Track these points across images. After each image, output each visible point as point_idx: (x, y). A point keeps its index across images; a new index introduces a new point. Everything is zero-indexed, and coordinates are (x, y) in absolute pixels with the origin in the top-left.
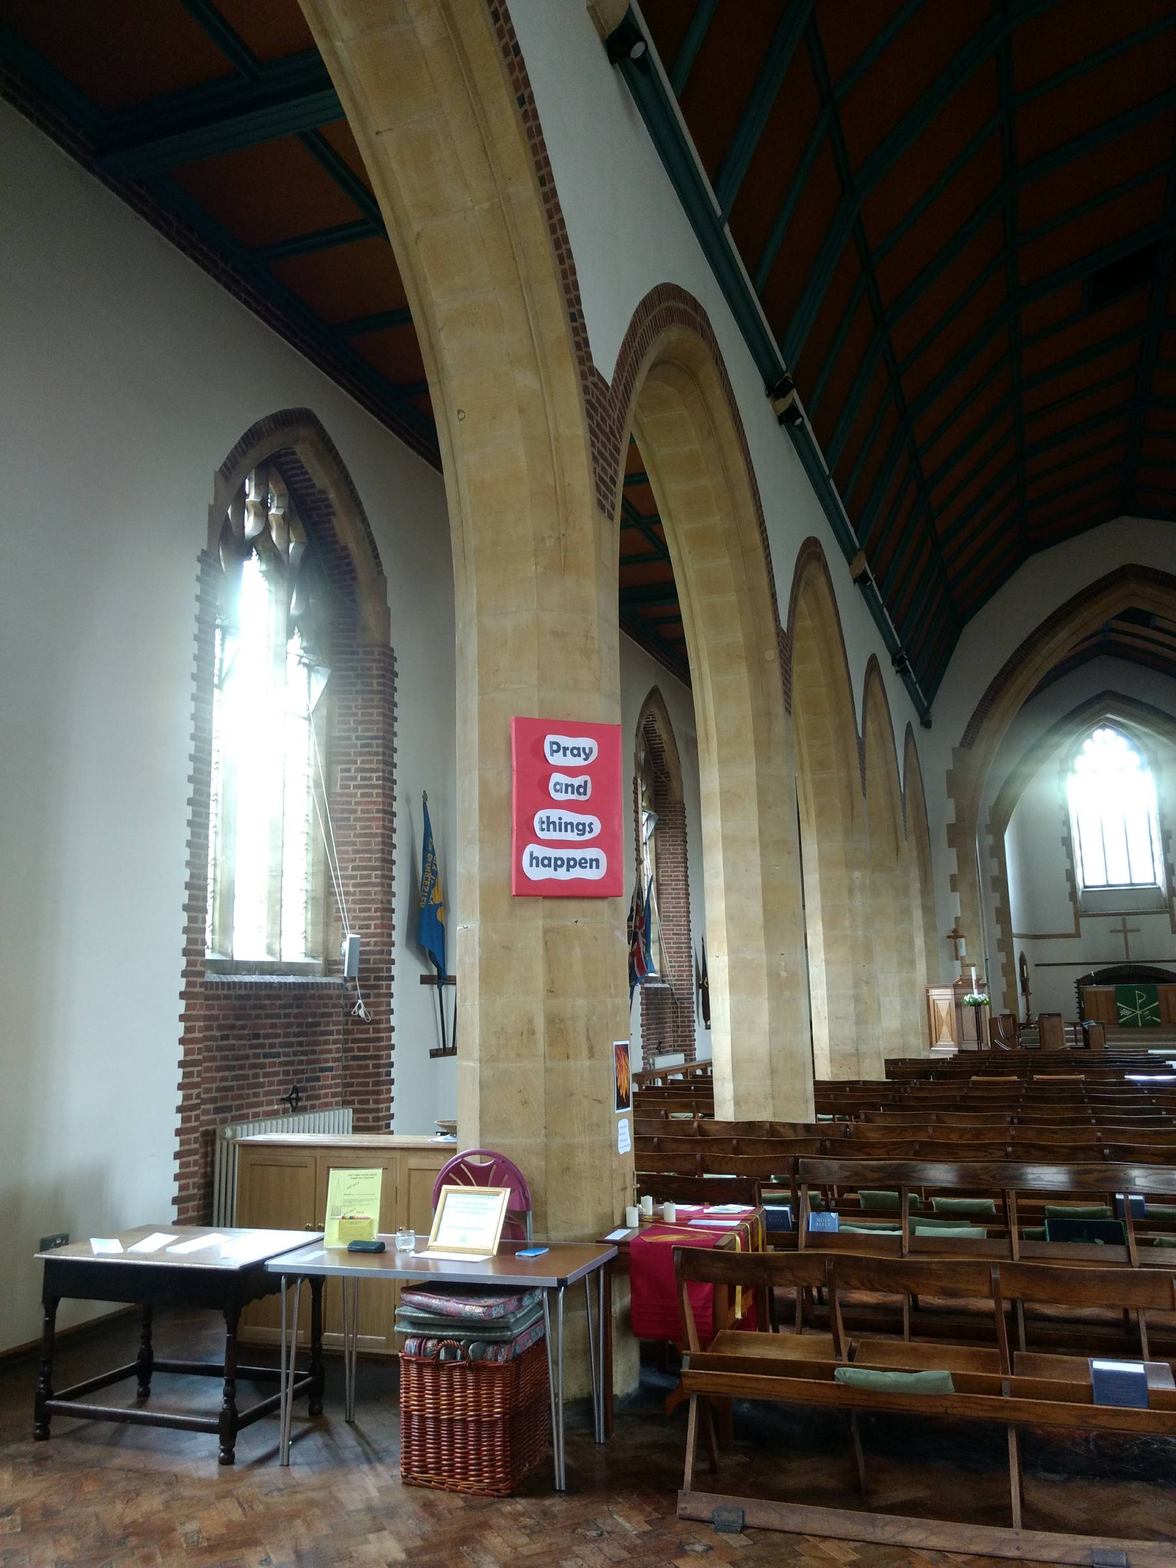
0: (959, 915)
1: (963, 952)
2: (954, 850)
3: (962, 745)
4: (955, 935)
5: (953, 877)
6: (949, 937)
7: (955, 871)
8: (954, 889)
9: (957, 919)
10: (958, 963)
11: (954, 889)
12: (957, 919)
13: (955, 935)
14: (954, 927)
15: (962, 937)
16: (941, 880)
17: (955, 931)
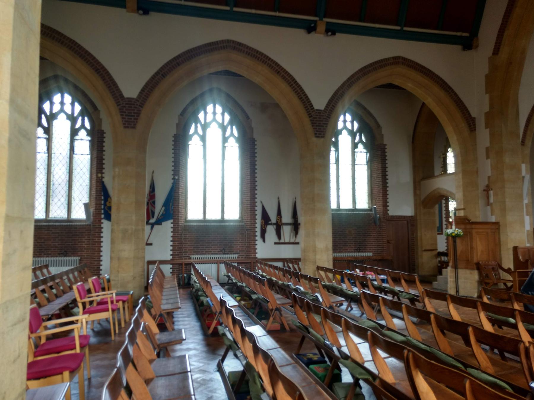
0: (490, 175)
1: (492, 200)
2: (488, 130)
3: (493, 54)
4: (487, 190)
5: (487, 149)
6: (484, 190)
7: (488, 144)
8: (488, 157)
9: (489, 177)
10: (489, 207)
11: (488, 157)
12: (489, 177)
13: (487, 190)
14: (487, 183)
15: (492, 189)
16: (481, 151)
17: (488, 186)
